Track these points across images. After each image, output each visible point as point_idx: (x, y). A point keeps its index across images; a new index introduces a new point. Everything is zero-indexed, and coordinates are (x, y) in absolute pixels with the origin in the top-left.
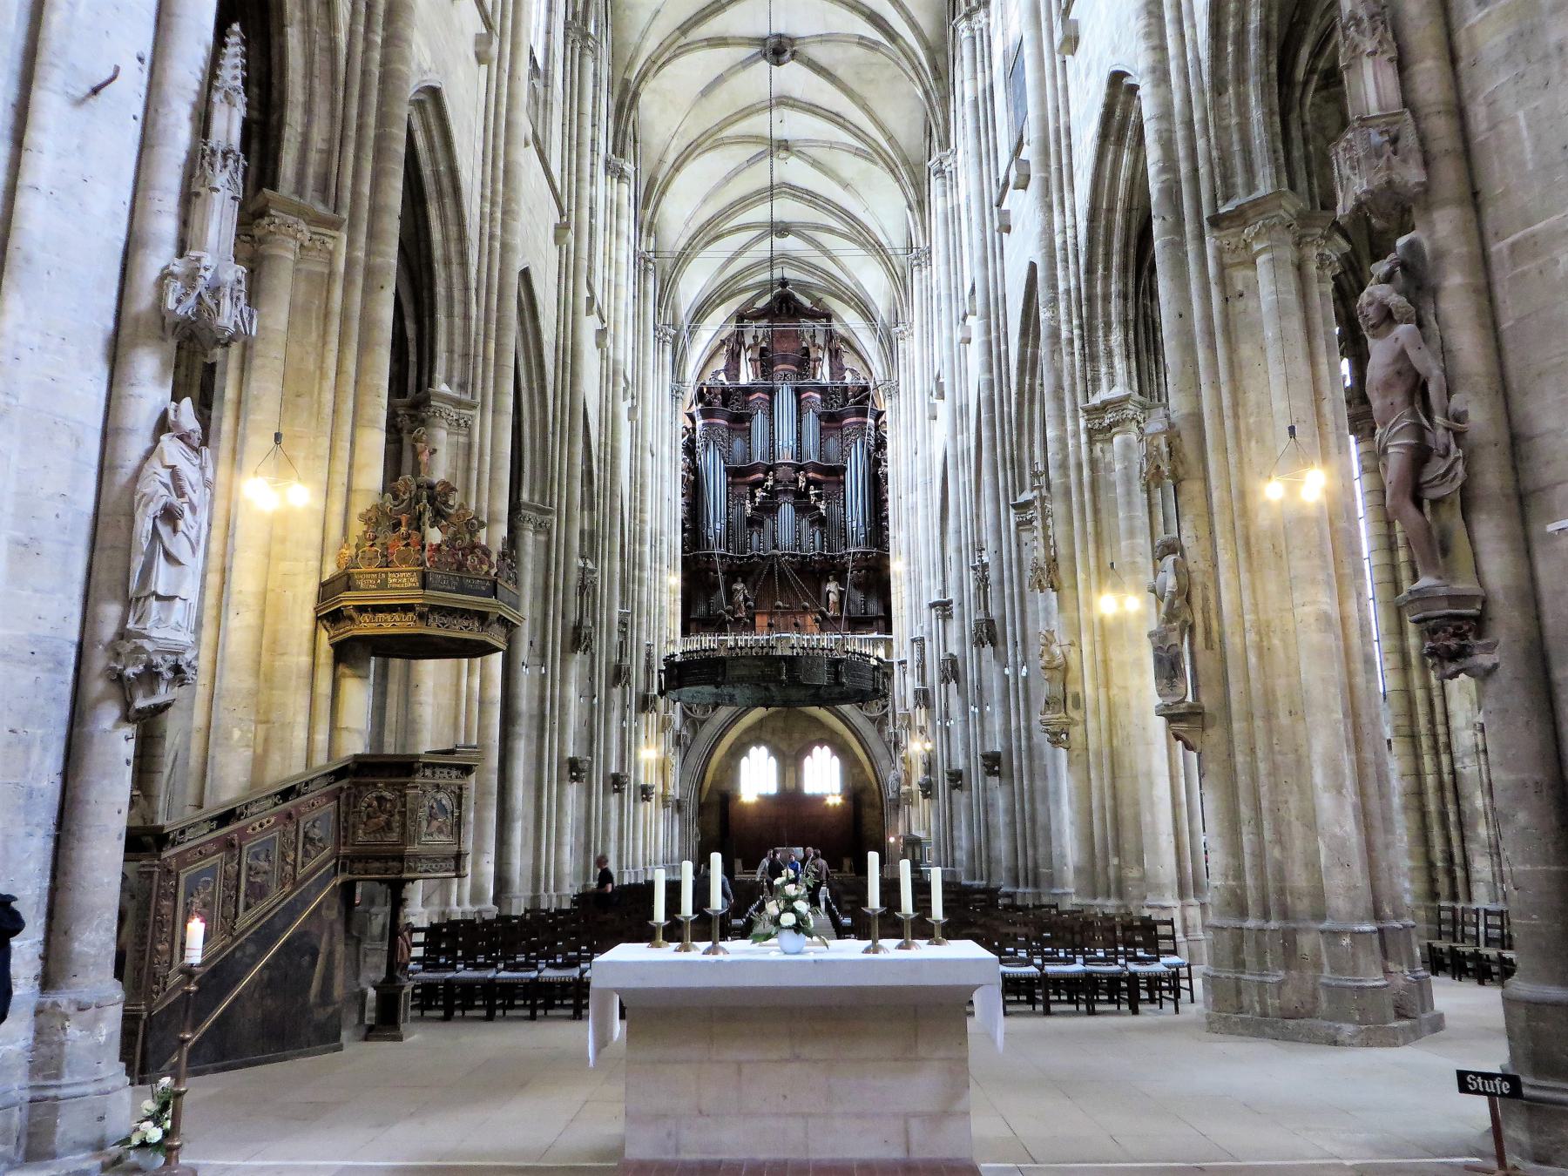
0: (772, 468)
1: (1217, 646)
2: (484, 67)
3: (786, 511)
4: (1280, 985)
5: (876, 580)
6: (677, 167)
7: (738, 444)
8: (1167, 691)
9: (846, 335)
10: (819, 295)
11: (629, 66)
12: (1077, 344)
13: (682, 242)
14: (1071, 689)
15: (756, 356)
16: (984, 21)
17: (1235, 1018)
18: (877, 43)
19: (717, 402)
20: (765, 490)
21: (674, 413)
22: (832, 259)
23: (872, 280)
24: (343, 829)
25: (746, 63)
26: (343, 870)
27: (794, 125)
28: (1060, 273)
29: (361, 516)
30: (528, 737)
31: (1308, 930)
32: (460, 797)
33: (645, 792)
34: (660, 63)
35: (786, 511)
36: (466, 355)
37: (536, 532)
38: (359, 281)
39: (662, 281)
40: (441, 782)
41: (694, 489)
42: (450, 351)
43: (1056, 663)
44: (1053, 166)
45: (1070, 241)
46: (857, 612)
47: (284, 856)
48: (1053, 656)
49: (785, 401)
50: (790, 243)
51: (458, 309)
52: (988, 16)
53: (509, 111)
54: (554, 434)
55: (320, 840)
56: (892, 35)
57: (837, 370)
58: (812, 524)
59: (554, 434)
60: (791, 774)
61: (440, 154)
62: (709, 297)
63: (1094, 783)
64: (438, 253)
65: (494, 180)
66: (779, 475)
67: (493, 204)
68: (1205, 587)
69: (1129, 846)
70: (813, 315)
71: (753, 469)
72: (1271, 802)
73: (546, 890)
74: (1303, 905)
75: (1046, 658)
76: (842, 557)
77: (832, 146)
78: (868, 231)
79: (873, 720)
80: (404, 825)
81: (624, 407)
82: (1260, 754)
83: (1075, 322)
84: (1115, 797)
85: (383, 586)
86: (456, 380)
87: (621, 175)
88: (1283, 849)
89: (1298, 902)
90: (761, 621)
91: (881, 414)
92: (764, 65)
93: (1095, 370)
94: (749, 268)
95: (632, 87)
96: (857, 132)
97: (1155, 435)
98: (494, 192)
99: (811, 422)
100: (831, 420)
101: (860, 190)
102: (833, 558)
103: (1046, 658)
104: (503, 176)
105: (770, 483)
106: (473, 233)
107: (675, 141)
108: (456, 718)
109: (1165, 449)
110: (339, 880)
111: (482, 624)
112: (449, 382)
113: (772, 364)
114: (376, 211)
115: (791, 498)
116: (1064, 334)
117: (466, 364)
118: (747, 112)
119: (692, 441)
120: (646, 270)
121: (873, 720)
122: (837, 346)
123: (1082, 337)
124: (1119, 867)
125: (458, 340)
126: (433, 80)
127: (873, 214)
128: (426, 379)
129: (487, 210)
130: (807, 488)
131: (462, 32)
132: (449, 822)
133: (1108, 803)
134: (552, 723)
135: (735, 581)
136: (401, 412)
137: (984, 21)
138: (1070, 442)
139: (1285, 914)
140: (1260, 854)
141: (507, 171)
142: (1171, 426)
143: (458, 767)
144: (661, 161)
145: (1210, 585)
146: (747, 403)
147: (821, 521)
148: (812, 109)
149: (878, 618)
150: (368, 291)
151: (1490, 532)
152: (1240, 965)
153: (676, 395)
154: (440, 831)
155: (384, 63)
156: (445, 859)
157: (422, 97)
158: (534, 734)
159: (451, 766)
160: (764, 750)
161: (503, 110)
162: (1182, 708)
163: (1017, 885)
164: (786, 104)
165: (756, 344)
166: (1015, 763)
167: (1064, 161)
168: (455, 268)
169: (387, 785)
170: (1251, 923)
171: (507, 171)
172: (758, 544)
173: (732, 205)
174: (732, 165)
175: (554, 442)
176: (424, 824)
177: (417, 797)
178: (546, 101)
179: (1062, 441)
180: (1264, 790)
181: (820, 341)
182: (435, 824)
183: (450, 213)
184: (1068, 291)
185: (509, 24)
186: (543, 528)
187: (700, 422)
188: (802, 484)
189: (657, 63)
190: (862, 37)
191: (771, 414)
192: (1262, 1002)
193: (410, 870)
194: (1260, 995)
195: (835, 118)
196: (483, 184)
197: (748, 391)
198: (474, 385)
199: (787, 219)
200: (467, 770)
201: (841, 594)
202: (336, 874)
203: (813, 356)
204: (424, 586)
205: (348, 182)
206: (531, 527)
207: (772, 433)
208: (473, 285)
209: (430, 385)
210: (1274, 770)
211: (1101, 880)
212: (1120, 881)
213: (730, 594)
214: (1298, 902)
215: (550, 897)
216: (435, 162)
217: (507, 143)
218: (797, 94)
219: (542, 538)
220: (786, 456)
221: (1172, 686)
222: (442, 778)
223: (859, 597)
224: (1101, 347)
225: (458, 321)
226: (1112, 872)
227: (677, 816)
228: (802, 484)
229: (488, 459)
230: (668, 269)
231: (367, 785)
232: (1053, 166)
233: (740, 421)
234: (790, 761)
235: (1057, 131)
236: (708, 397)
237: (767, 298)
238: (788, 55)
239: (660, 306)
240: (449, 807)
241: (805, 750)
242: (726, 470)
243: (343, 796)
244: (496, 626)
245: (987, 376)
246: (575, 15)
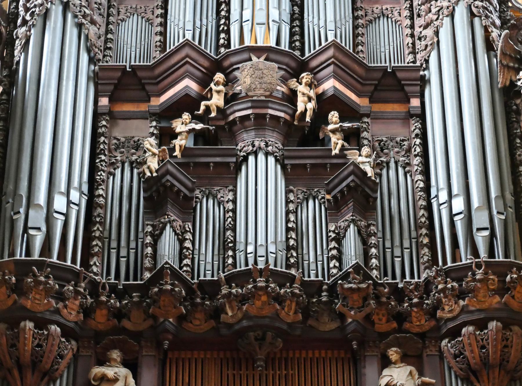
3: (262, 182)
35: (262, 182)
58: (335, 208)
66: (245, 78)
76: (427, 286)
102: (399, 294)
115: (274, 140)
130: (320, 117)
135: (103, 361)
228: (305, 105)
242: (96, 79)
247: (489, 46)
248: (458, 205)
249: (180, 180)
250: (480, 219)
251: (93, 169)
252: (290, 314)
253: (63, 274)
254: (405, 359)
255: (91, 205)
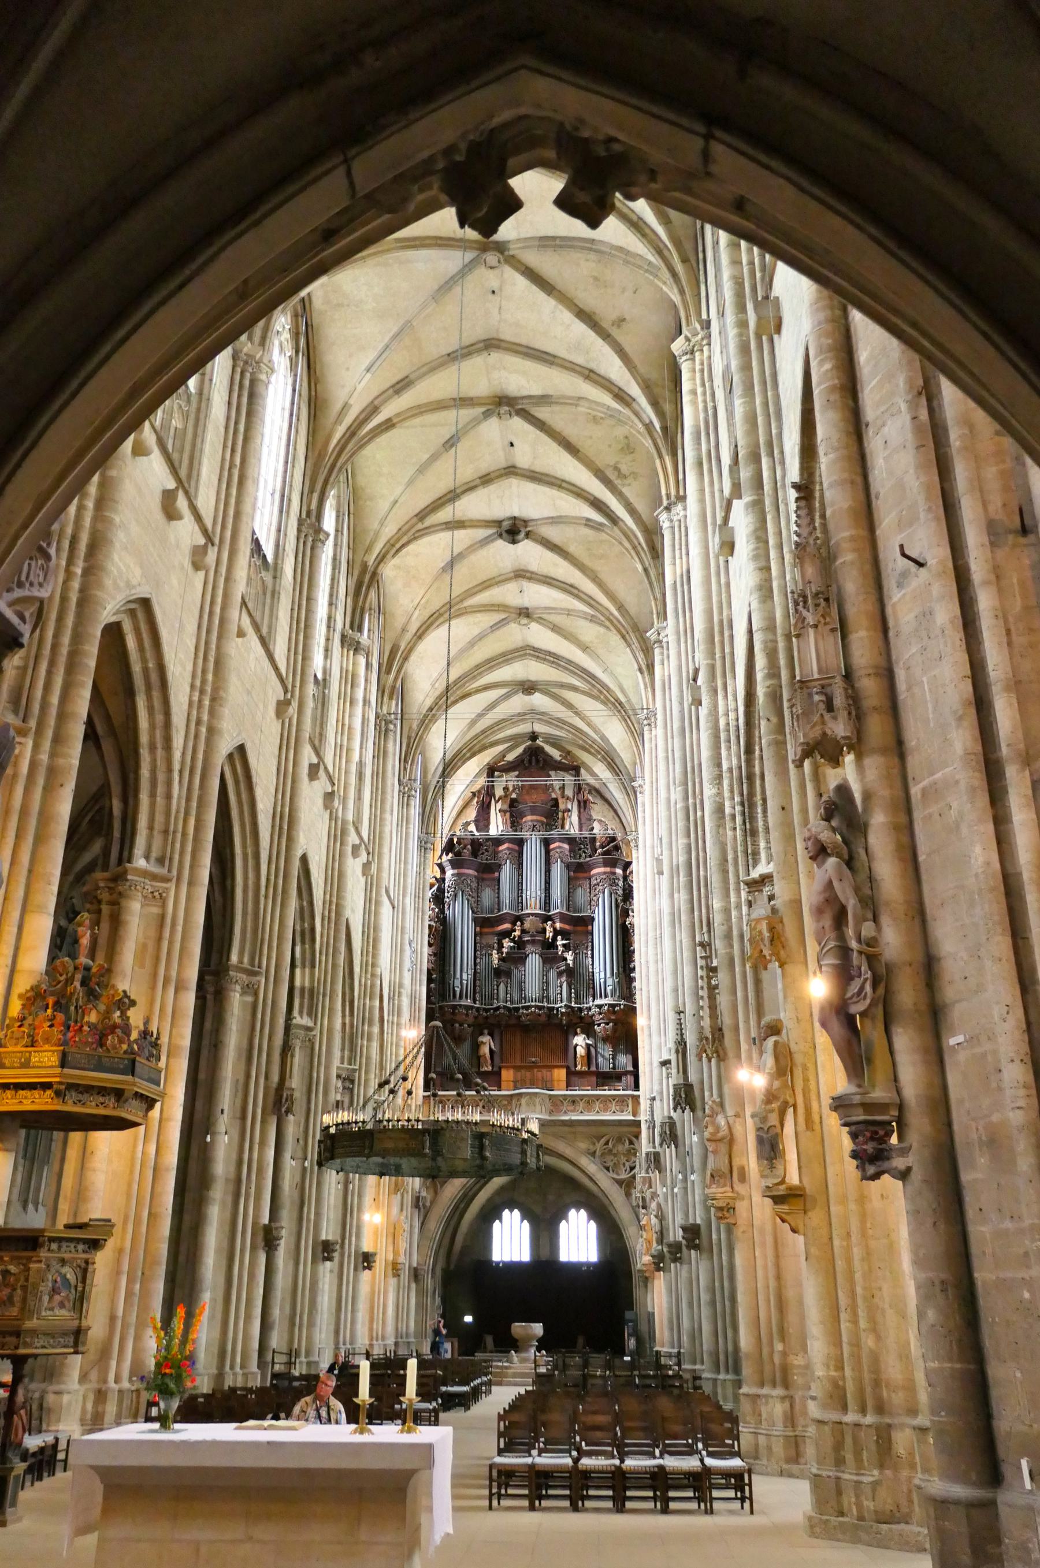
0: (520, 918)
1: (817, 1127)
2: (201, 574)
3: (534, 962)
4: (875, 1484)
5: (624, 1035)
6: (420, 635)
7: (487, 895)
8: (767, 1172)
9: (597, 786)
10: (569, 748)
11: (368, 550)
12: (739, 819)
13: (429, 702)
14: (737, 1162)
15: (506, 807)
16: (682, 513)
17: (834, 1520)
18: (601, 524)
19: (466, 853)
20: (513, 940)
21: (422, 864)
22: (577, 713)
23: (615, 733)
25: (485, 542)
27: (536, 596)
28: (724, 753)
29: (20, 996)
30: (223, 1203)
31: (902, 1426)
32: (85, 1271)
33: (367, 1260)
34: (398, 546)
35: (534, 962)
36: (166, 832)
37: (243, 993)
38: (41, 781)
39: (409, 738)
40: (67, 1256)
41: (441, 937)
42: (151, 828)
43: (720, 1135)
44: (718, 655)
45: (732, 723)
46: (605, 1066)
48: (718, 1129)
49: (533, 851)
50: (539, 700)
51: (160, 789)
52: (685, 509)
53: (223, 609)
54: (266, 897)
56: (614, 519)
57: (585, 820)
58: (560, 974)
59: (266, 897)
60: (544, 1241)
61: (149, 654)
62: (460, 751)
63: (759, 1263)
64: (144, 739)
65: (204, 671)
66: (527, 925)
67: (202, 692)
68: (805, 1068)
69: (792, 1330)
70: (559, 767)
71: (501, 919)
72: (865, 1289)
73: (232, 1367)
74: (898, 1399)
75: (710, 1129)
76: (590, 1009)
77: (569, 612)
78: (609, 690)
79: (620, 1183)
80: (24, 1300)
81: (354, 867)
82: (854, 1239)
83: (737, 799)
84: (778, 1277)
85: (26, 1064)
86: (154, 855)
87: (357, 648)
88: (878, 1338)
89: (893, 1395)
90: (507, 1075)
91: (629, 864)
92: (500, 544)
93: (755, 844)
94: (497, 723)
95: (371, 569)
96: (589, 601)
97: (758, 921)
98: (204, 682)
99: (558, 871)
100: (577, 871)
101: (600, 652)
102: (580, 1010)
103: (710, 1129)
104: (213, 667)
105: (517, 933)
106: (179, 719)
107: (417, 612)
108: (129, 1186)
109: (766, 934)
111: (118, 1101)
112: (147, 857)
113: (522, 815)
114: (63, 716)
115: (539, 950)
116: (728, 810)
117: (166, 840)
118: (487, 585)
119: (441, 890)
120: (387, 731)
121: (620, 1183)
122: (587, 796)
123: (743, 813)
124: (784, 1354)
125: (159, 818)
126: (143, 592)
127: (612, 674)
128: (126, 854)
129: (196, 698)
130: (555, 939)
131: (178, 546)
132: (72, 1297)
133: (772, 1283)
134: (248, 1188)
135: (482, 1034)
136: (102, 884)
137: (682, 513)
138: (734, 913)
139: (880, 1409)
140: (856, 1344)
141: (218, 663)
142: (774, 910)
143: (85, 1241)
144: (404, 630)
145: (810, 1066)
146: (496, 853)
147: (571, 973)
148: (548, 581)
149: (626, 1073)
150: (49, 789)
151: (906, 1042)
152: (840, 1462)
153: (424, 846)
154: (62, 1305)
155: (83, 590)
156: (64, 1334)
157: (133, 606)
158: (229, 1199)
159: (78, 1240)
160: (516, 1213)
161: (218, 610)
162: (782, 1190)
163: (718, 1372)
164: (524, 577)
165: (506, 796)
166: (714, 1236)
167: (727, 650)
168: (160, 752)
169: (12, 1259)
170: (850, 1418)
171: (218, 663)
172: (503, 995)
173: (478, 667)
174: (476, 631)
175: (266, 905)
176: (46, 1298)
177: (39, 1271)
178: (273, 592)
179: (727, 911)
180: (858, 1276)
181: (569, 792)
182: (57, 1298)
183: (157, 703)
184: (730, 770)
185: (228, 534)
186: (251, 990)
187: (450, 872)
188: (549, 934)
189: (395, 547)
190: (588, 520)
191: (520, 865)
192: (859, 1505)
193: (26, 1345)
194: (857, 1496)
195: (570, 589)
196: (194, 677)
197: (497, 841)
198: (171, 859)
199: (533, 678)
200: (95, 1245)
201: (588, 1046)
203: (562, 807)
204: (63, 1065)
205: (39, 693)
206: (238, 988)
207: (520, 883)
208: (176, 766)
209: (129, 861)
210: (868, 1255)
211: (767, 1368)
212: (785, 1369)
213: (476, 1046)
214: (893, 1395)
215: (235, 1374)
216: (144, 660)
217: (220, 637)
218: (534, 567)
219: (249, 999)
220: (533, 905)
221: (772, 1167)
222: (67, 1252)
223: (606, 1051)
224: (760, 823)
225: (160, 800)
226: (777, 1359)
227: (413, 1286)
228: (549, 934)
229: (180, 928)
230: (415, 726)
232: (718, 655)
233: (489, 871)
234: (545, 1229)
235: (721, 622)
236: (457, 848)
237: (520, 750)
238: (522, 535)
239: (406, 761)
240: (73, 1281)
241: (561, 1214)
242: (475, 920)
244: (135, 1103)
245: (685, 841)
246: (309, 513)
247: (617, 906)
248: (602, 975)
249: (505, 966)
250: (609, 982)
251: (475, 958)
252: (543, 1019)
253: (468, 1008)
254: (583, 1032)
255: (475, 973)
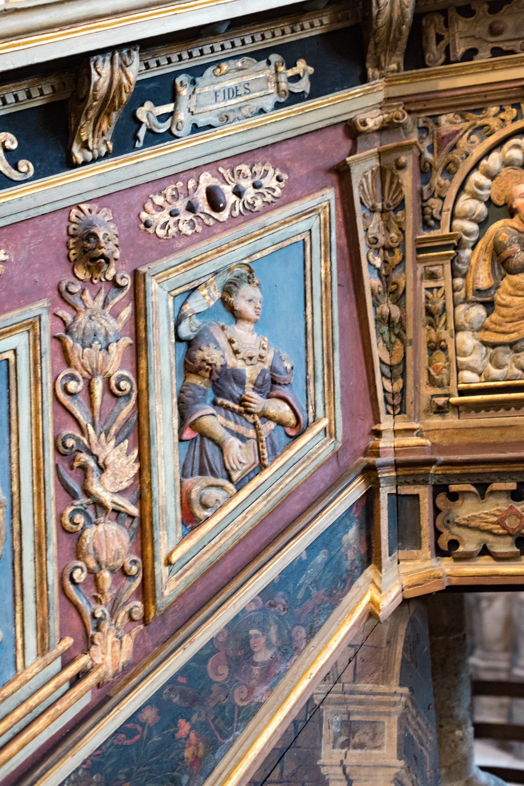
24: (382, 327)
26: (406, 535)
47: (73, 465)
55: (271, 383)
110: (387, 586)
202: (370, 556)
231: (471, 104)
243: (363, 168)
